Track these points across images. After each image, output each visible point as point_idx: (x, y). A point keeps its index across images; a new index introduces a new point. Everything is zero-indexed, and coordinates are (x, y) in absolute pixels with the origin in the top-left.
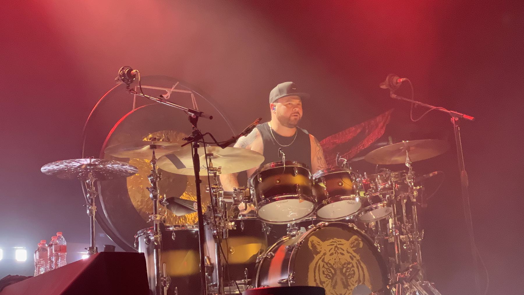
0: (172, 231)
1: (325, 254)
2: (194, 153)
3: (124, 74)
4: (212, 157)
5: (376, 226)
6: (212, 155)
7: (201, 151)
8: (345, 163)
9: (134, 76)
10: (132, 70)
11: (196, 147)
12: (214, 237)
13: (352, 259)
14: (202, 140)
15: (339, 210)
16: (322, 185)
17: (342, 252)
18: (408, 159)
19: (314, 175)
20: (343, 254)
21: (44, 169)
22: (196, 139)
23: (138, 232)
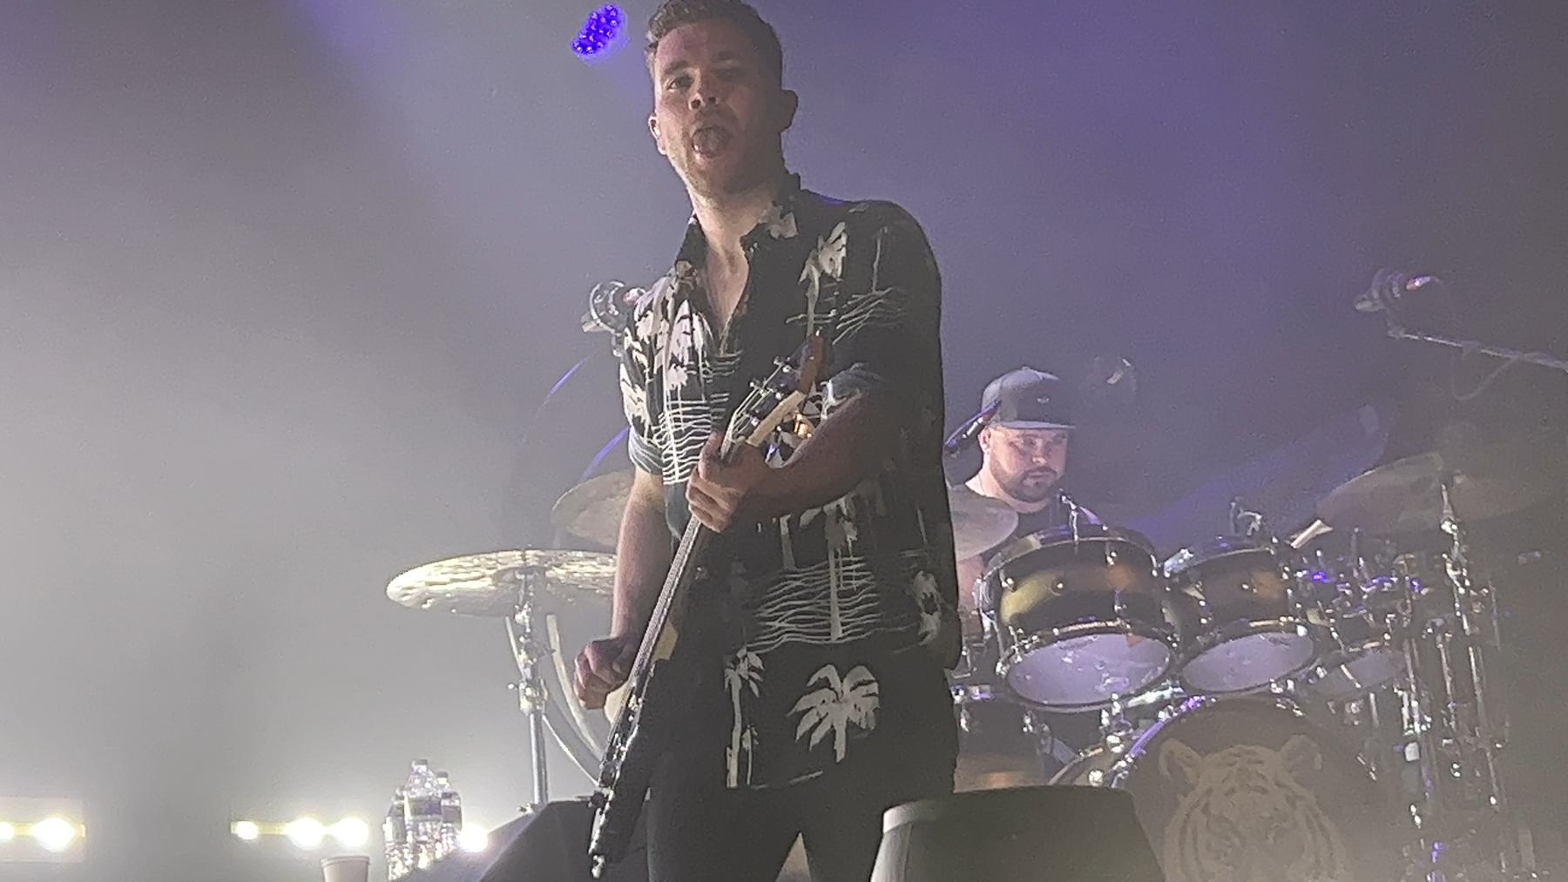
1: (1209, 791)
13: (1293, 805)
17: (1261, 783)
19: (1167, 564)
20: (1264, 791)
21: (394, 588)
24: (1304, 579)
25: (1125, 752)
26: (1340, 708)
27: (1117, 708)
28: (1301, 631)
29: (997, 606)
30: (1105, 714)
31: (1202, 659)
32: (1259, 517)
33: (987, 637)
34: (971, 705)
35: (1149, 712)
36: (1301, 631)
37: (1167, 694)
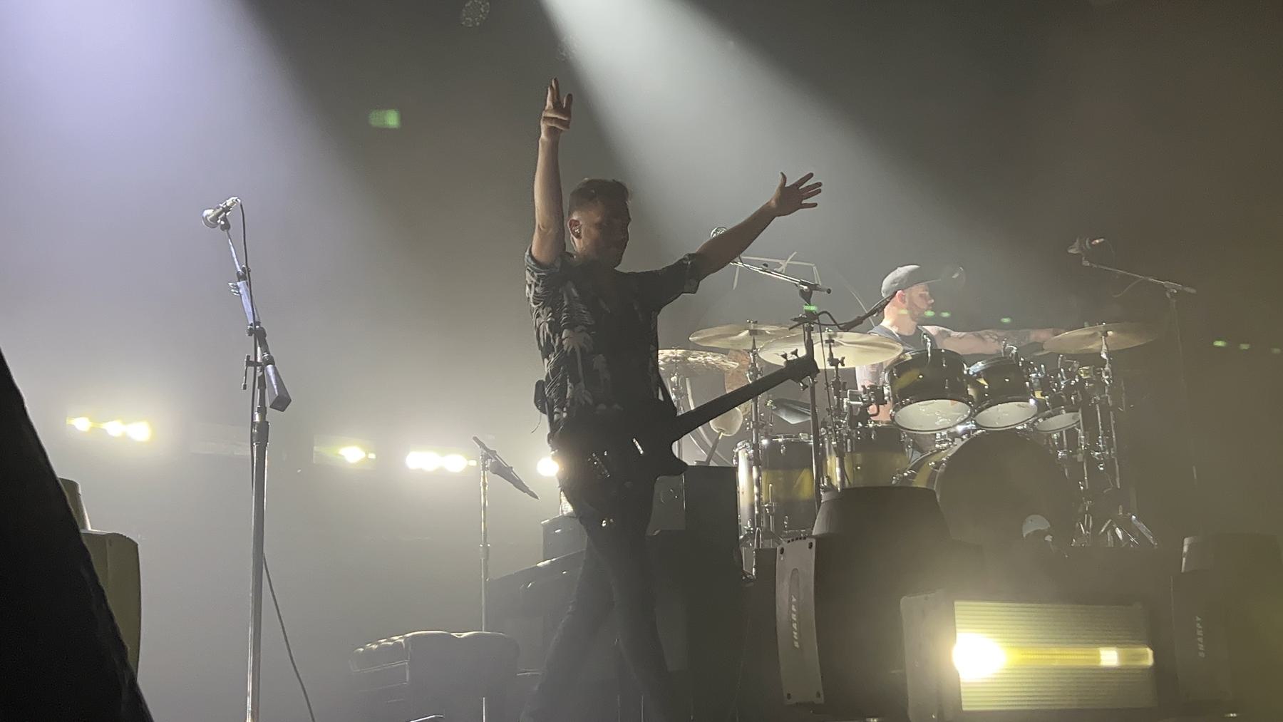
5: (1060, 439)
7: (815, 336)
11: (810, 330)
15: (1007, 415)
16: (982, 381)
18: (1104, 348)
22: (809, 322)
27: (944, 433)
28: (1032, 402)
34: (876, 428)
35: (960, 436)
36: (1032, 402)
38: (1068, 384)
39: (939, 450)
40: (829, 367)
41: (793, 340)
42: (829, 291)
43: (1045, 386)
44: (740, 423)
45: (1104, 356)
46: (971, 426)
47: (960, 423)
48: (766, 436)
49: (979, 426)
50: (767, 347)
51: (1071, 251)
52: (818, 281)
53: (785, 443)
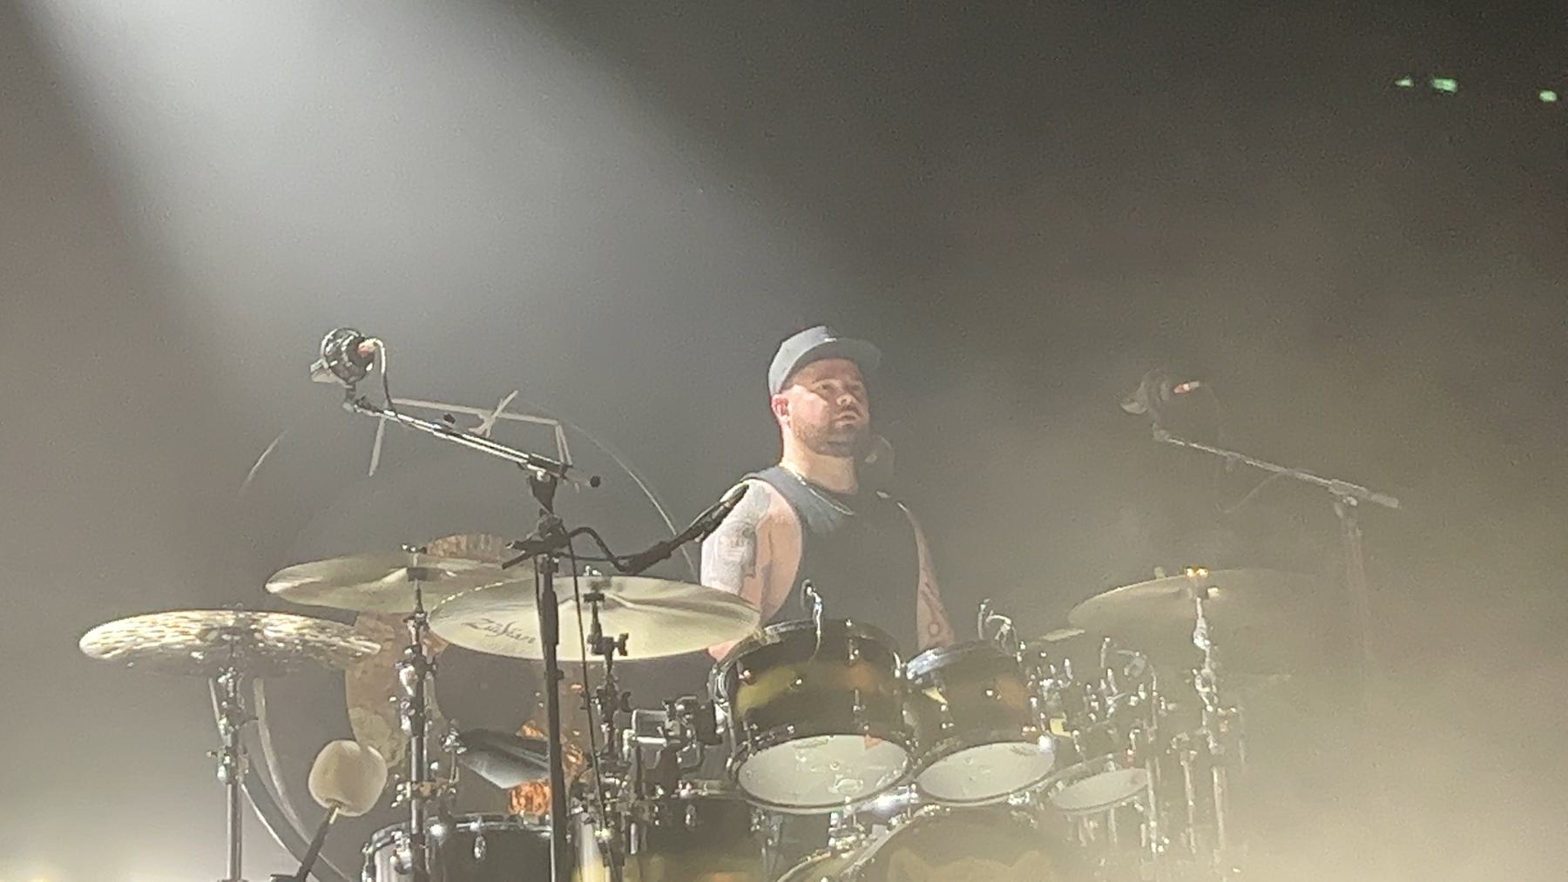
0: (474, 834)
2: (541, 590)
3: (337, 353)
4: (599, 604)
6: (602, 597)
8: (1005, 628)
9: (371, 357)
10: (363, 340)
11: (550, 571)
12: (603, 848)
14: (566, 550)
16: (935, 695)
21: (92, 641)
23: (375, 837)
24: (1049, 691)
25: (854, 859)
26: (1077, 823)
27: (848, 810)
28: (1045, 743)
29: (732, 699)
30: (834, 816)
31: (940, 764)
32: (1008, 621)
33: (720, 730)
34: (695, 800)
35: (883, 819)
37: (904, 798)
38: (1122, 703)
39: (836, 853)
40: (590, 657)
41: (511, 592)
42: (595, 482)
43: (1071, 706)
44: (380, 784)
45: (1200, 642)
46: (909, 796)
47: (888, 789)
48: (444, 819)
49: (926, 798)
50: (451, 609)
51: (1127, 408)
52: (564, 456)
53: (487, 834)
